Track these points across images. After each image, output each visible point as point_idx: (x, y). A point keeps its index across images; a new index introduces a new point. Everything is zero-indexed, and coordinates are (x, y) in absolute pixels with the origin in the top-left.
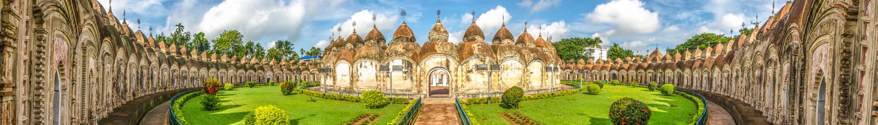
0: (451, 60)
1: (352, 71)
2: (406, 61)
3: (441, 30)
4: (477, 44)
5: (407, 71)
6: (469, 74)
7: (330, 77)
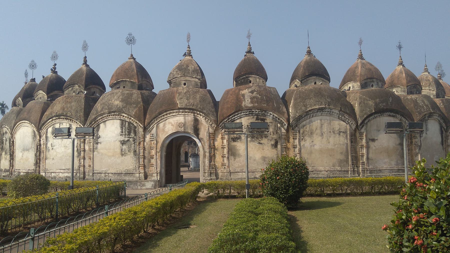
0: (201, 118)
1: (40, 141)
2: (126, 121)
3: (189, 68)
4: (250, 90)
5: (128, 140)
6: (235, 143)
7: (6, 153)
